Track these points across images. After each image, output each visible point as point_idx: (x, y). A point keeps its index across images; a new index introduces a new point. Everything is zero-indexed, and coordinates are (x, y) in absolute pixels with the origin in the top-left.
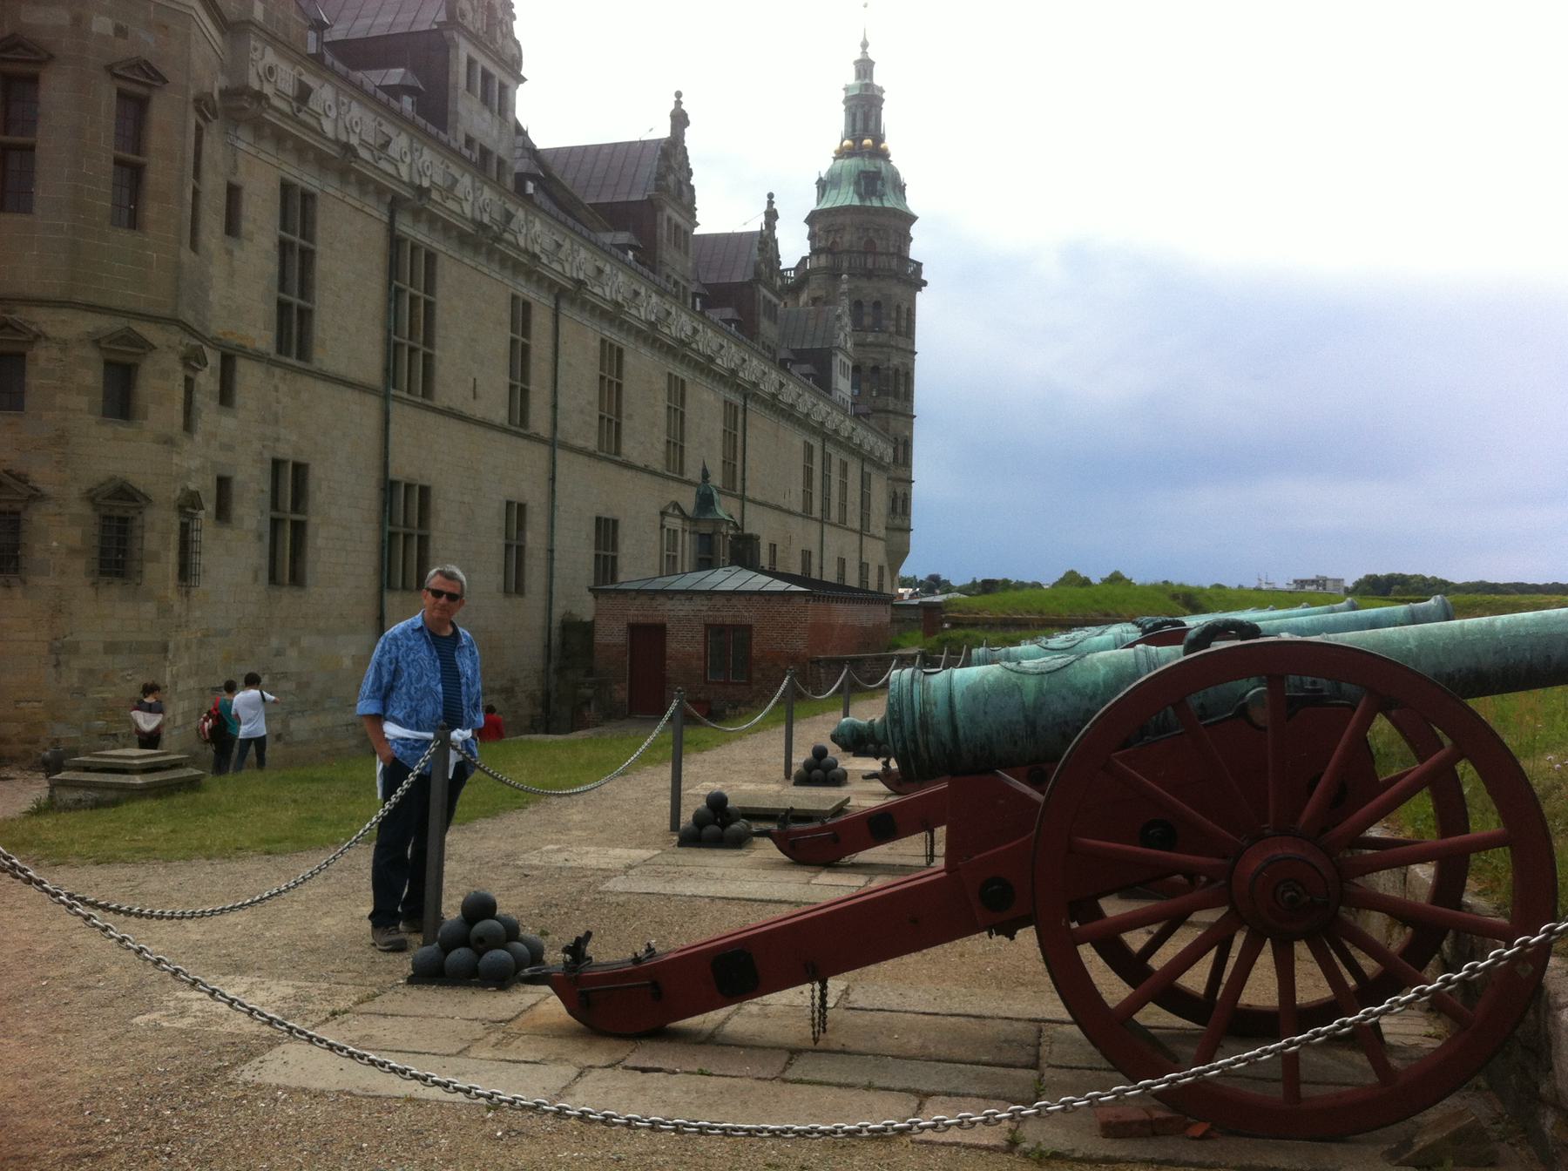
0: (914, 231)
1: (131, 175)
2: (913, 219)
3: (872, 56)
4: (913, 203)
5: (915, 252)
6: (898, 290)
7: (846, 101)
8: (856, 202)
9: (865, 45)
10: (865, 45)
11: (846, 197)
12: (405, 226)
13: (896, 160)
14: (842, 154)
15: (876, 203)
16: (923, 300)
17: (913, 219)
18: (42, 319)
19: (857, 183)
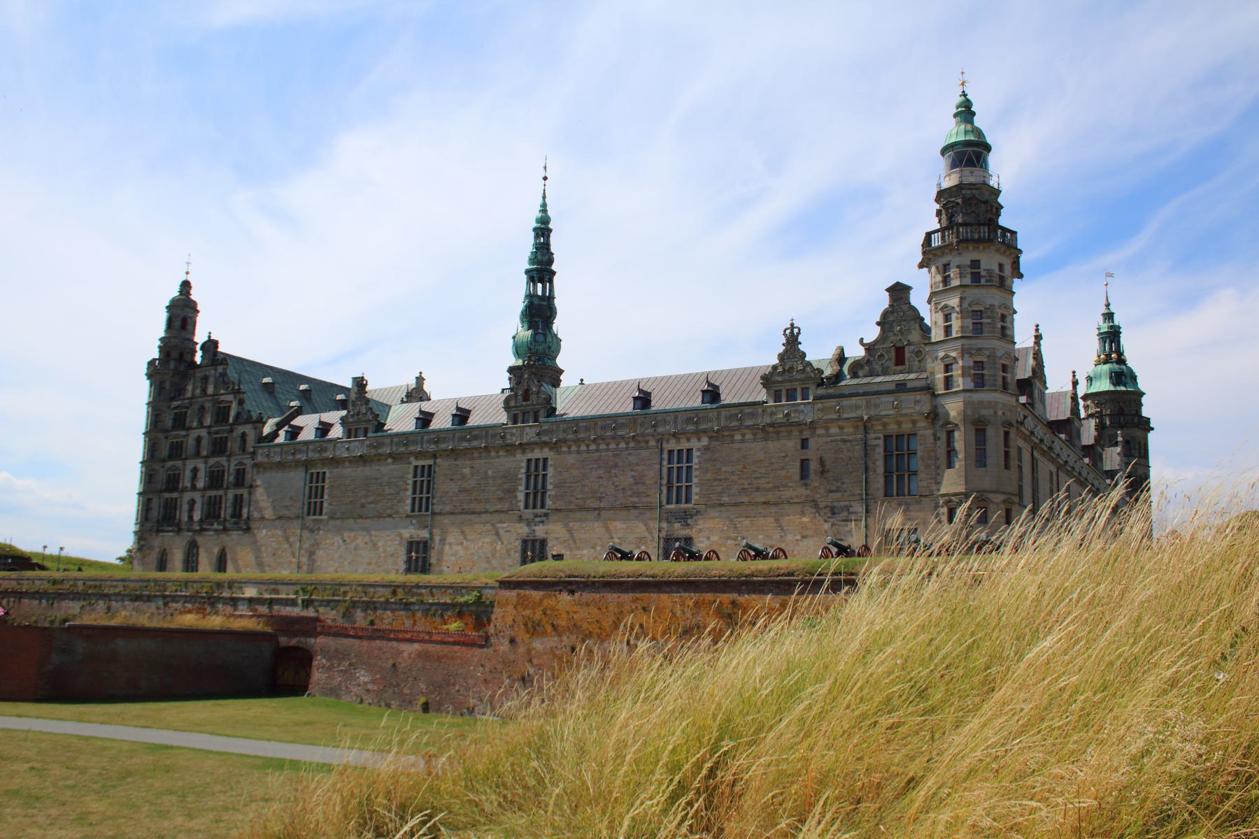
0: (1143, 400)
1: (1007, 454)
2: (1142, 394)
3: (1112, 309)
4: (1142, 386)
5: (1145, 413)
6: (1138, 433)
7: (1100, 334)
8: (1112, 388)
9: (1108, 305)
10: (1108, 305)
11: (1104, 385)
12: (1036, 454)
13: (1130, 363)
14: (1098, 363)
15: (1123, 388)
16: (1151, 435)
17: (1142, 394)
18: (991, 496)
19: (1111, 378)
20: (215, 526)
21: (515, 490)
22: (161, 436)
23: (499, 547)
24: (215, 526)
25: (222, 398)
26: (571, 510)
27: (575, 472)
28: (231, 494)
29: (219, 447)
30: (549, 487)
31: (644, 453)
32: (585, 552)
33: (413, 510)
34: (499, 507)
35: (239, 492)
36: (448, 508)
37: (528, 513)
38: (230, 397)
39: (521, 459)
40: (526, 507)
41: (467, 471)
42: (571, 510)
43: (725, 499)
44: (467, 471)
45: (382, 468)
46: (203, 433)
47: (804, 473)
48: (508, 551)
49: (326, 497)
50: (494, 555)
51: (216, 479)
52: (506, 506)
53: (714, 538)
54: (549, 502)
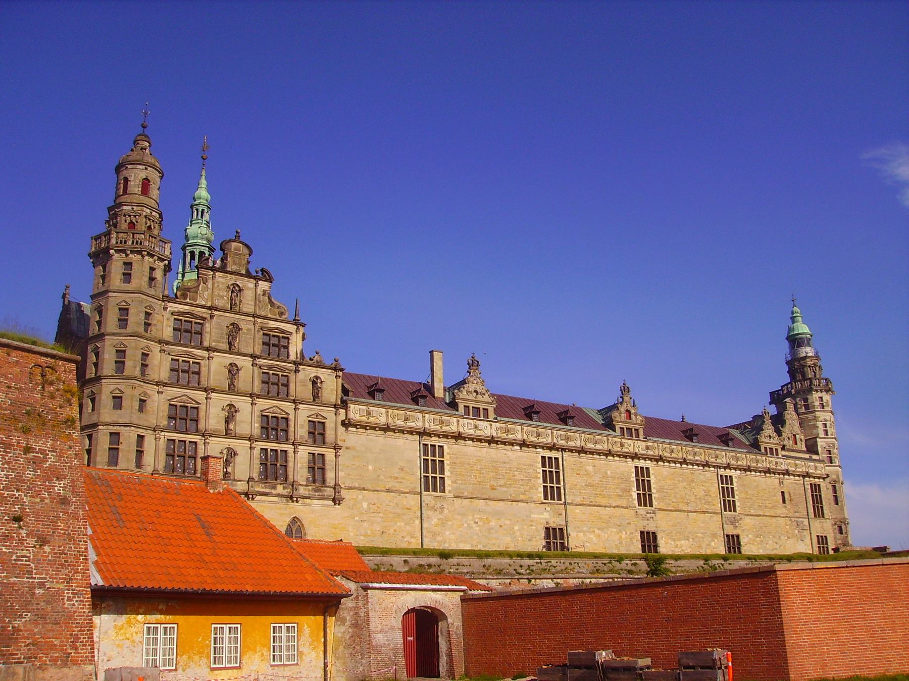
20: (280, 489)
21: (630, 490)
22: (156, 348)
23: (623, 536)
24: (280, 489)
25: (272, 324)
26: (670, 510)
27: (669, 482)
28: (303, 453)
29: (275, 386)
30: (653, 491)
31: (708, 475)
32: (683, 542)
33: (546, 498)
34: (619, 503)
35: (318, 450)
36: (578, 500)
37: (642, 510)
38: (291, 328)
39: (631, 465)
40: (640, 505)
41: (590, 468)
42: (670, 510)
43: (752, 512)
44: (590, 468)
45: (510, 453)
46: (244, 363)
47: (784, 502)
48: (631, 539)
49: (447, 473)
50: (621, 543)
51: (273, 427)
52: (624, 503)
53: (750, 536)
54: (655, 503)
